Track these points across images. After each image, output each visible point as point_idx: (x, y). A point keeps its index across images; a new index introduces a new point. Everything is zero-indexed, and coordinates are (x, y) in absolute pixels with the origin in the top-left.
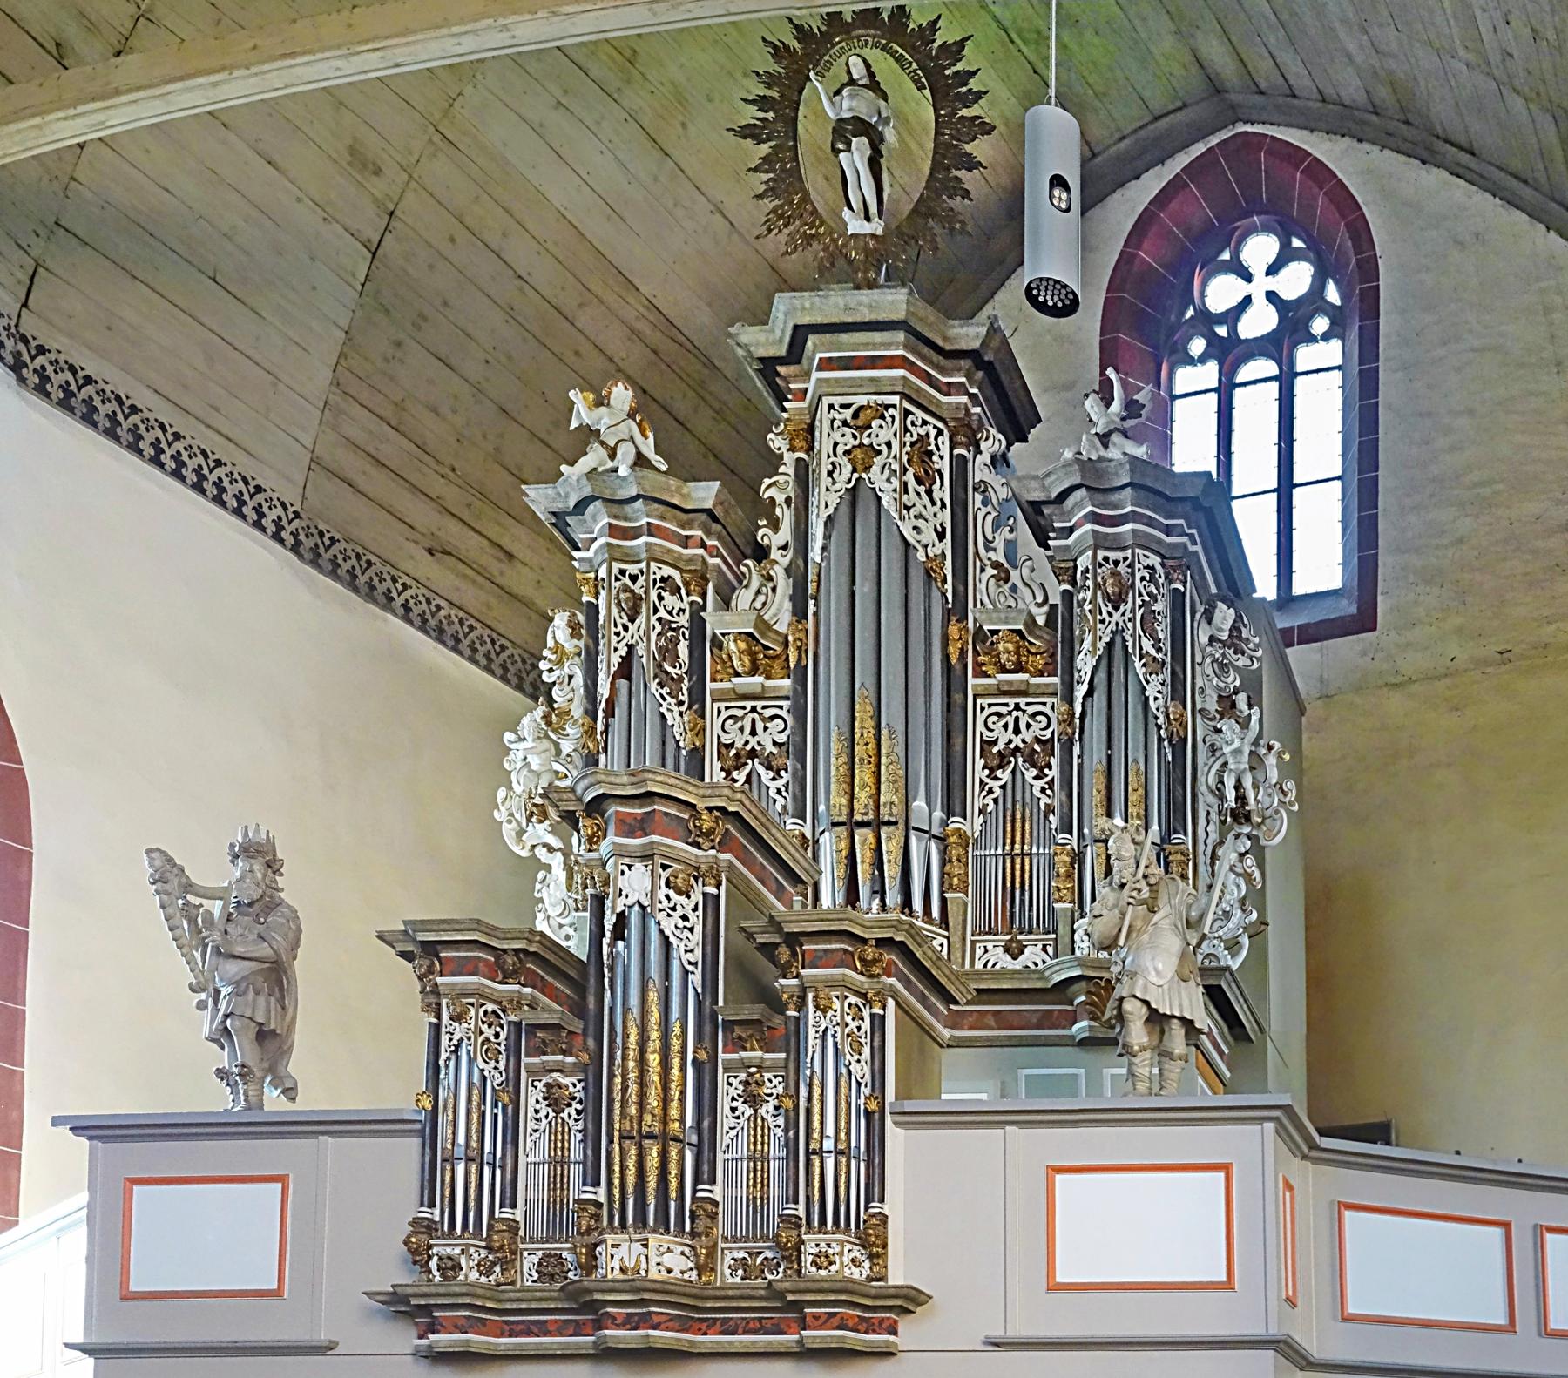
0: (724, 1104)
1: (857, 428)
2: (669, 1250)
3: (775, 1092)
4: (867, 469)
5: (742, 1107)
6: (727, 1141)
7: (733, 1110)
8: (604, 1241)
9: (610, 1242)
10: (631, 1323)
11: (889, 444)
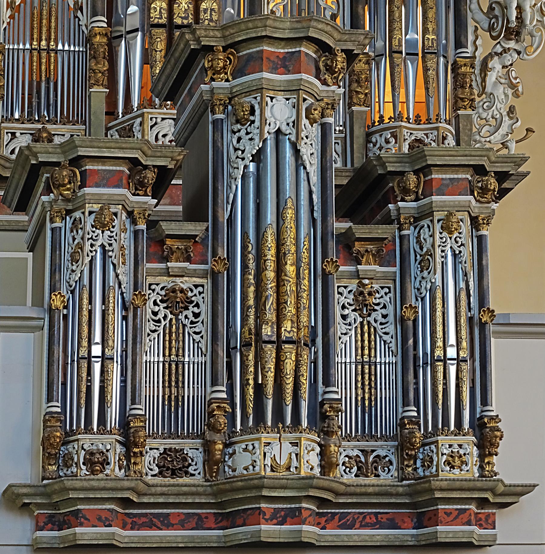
0: (338, 311)
5: (353, 315)
7: (344, 317)
10: (281, 518)
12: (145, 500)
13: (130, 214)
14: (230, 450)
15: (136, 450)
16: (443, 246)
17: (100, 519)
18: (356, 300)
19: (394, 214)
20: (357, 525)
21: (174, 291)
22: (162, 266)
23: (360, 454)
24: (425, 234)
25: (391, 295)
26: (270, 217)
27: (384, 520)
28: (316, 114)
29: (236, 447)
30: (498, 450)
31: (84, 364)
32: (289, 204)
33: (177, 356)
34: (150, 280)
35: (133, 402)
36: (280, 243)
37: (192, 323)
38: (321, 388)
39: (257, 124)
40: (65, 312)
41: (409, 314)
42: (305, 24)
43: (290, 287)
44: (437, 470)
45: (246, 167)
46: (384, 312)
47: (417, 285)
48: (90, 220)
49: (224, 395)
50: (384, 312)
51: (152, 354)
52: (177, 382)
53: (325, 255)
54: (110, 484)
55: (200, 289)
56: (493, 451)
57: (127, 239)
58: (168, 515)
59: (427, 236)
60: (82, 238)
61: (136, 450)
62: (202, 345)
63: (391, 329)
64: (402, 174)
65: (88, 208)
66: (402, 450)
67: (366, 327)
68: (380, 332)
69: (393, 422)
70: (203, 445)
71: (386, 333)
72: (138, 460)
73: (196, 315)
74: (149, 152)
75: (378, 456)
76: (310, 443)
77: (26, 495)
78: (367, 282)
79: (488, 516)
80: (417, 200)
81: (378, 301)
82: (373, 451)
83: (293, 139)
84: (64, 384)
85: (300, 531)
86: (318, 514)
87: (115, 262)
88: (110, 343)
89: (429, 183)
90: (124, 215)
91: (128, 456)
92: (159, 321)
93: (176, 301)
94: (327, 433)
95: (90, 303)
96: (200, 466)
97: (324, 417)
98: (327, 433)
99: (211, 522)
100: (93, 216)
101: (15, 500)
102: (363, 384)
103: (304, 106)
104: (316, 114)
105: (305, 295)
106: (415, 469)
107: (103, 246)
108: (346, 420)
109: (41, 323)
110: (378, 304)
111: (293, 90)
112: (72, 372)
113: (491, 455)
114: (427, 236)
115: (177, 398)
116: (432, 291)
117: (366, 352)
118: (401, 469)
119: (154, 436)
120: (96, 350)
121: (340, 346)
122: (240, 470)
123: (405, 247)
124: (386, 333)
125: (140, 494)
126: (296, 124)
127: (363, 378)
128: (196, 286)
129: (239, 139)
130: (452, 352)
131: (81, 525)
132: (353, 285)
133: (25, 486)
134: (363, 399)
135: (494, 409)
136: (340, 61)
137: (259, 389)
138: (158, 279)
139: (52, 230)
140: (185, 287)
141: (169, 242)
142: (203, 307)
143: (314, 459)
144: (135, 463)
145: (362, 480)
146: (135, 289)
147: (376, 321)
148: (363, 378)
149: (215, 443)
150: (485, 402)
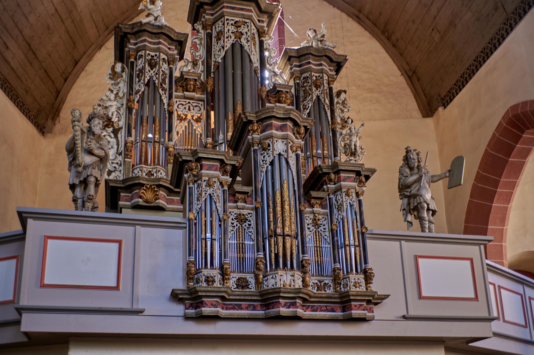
0: (306, 226)
5: (312, 228)
7: (309, 229)
8: (277, 273)
9: (280, 274)
12: (231, 297)
13: (221, 183)
14: (266, 279)
15: (227, 277)
16: (346, 201)
17: (212, 305)
18: (313, 222)
19: (326, 189)
20: (319, 310)
21: (240, 215)
22: (235, 205)
24: (339, 197)
25: (327, 221)
28: (294, 149)
29: (269, 277)
30: (373, 281)
31: (204, 241)
32: (285, 182)
33: (242, 241)
34: (230, 210)
35: (225, 258)
38: (301, 256)
39: (271, 150)
40: (195, 221)
41: (334, 227)
42: (289, 112)
43: (287, 214)
44: (350, 288)
45: (267, 167)
46: (324, 227)
47: (337, 217)
48: (204, 184)
49: (262, 256)
50: (324, 227)
51: (232, 241)
52: (243, 252)
53: (300, 203)
54: (216, 289)
55: (251, 215)
56: (371, 281)
57: (220, 193)
58: (241, 305)
59: (340, 198)
60: (201, 191)
61: (227, 277)
62: (252, 237)
63: (327, 234)
64: (328, 174)
65: (203, 178)
66: (335, 281)
67: (317, 233)
68: (323, 235)
69: (330, 270)
70: (255, 277)
72: (228, 281)
74: (228, 158)
75: (325, 283)
76: (298, 275)
77: (181, 294)
79: (370, 308)
80: (335, 184)
83: (286, 156)
84: (196, 251)
85: (296, 311)
86: (302, 306)
87: (215, 200)
88: (214, 233)
89: (339, 178)
90: (219, 184)
91: (223, 279)
92: (234, 227)
93: (241, 219)
94: (305, 273)
95: (205, 217)
96: (254, 285)
97: (303, 266)
98: (305, 273)
99: (259, 307)
100: (206, 182)
101: (175, 297)
102: (317, 255)
103: (290, 145)
104: (294, 149)
105: (293, 218)
106: (340, 288)
107: (210, 194)
108: (311, 268)
109: (185, 225)
112: (199, 244)
113: (370, 283)
114: (340, 198)
115: (243, 258)
116: (343, 219)
117: (318, 242)
118: (335, 288)
119: (234, 272)
120: (209, 235)
121: (307, 240)
122: (270, 286)
123: (331, 202)
125: (229, 295)
126: (287, 151)
127: (317, 253)
128: (249, 214)
129: (264, 157)
130: (352, 242)
131: (204, 307)
132: (312, 216)
133: (179, 290)
134: (318, 261)
135: (370, 266)
136: (302, 130)
137: (277, 255)
138: (233, 210)
139: (189, 188)
140: (244, 213)
141: (237, 195)
142: (252, 222)
143: (301, 283)
144: (226, 283)
145: (319, 292)
146: (224, 212)
148: (317, 253)
149: (259, 275)
150: (366, 263)
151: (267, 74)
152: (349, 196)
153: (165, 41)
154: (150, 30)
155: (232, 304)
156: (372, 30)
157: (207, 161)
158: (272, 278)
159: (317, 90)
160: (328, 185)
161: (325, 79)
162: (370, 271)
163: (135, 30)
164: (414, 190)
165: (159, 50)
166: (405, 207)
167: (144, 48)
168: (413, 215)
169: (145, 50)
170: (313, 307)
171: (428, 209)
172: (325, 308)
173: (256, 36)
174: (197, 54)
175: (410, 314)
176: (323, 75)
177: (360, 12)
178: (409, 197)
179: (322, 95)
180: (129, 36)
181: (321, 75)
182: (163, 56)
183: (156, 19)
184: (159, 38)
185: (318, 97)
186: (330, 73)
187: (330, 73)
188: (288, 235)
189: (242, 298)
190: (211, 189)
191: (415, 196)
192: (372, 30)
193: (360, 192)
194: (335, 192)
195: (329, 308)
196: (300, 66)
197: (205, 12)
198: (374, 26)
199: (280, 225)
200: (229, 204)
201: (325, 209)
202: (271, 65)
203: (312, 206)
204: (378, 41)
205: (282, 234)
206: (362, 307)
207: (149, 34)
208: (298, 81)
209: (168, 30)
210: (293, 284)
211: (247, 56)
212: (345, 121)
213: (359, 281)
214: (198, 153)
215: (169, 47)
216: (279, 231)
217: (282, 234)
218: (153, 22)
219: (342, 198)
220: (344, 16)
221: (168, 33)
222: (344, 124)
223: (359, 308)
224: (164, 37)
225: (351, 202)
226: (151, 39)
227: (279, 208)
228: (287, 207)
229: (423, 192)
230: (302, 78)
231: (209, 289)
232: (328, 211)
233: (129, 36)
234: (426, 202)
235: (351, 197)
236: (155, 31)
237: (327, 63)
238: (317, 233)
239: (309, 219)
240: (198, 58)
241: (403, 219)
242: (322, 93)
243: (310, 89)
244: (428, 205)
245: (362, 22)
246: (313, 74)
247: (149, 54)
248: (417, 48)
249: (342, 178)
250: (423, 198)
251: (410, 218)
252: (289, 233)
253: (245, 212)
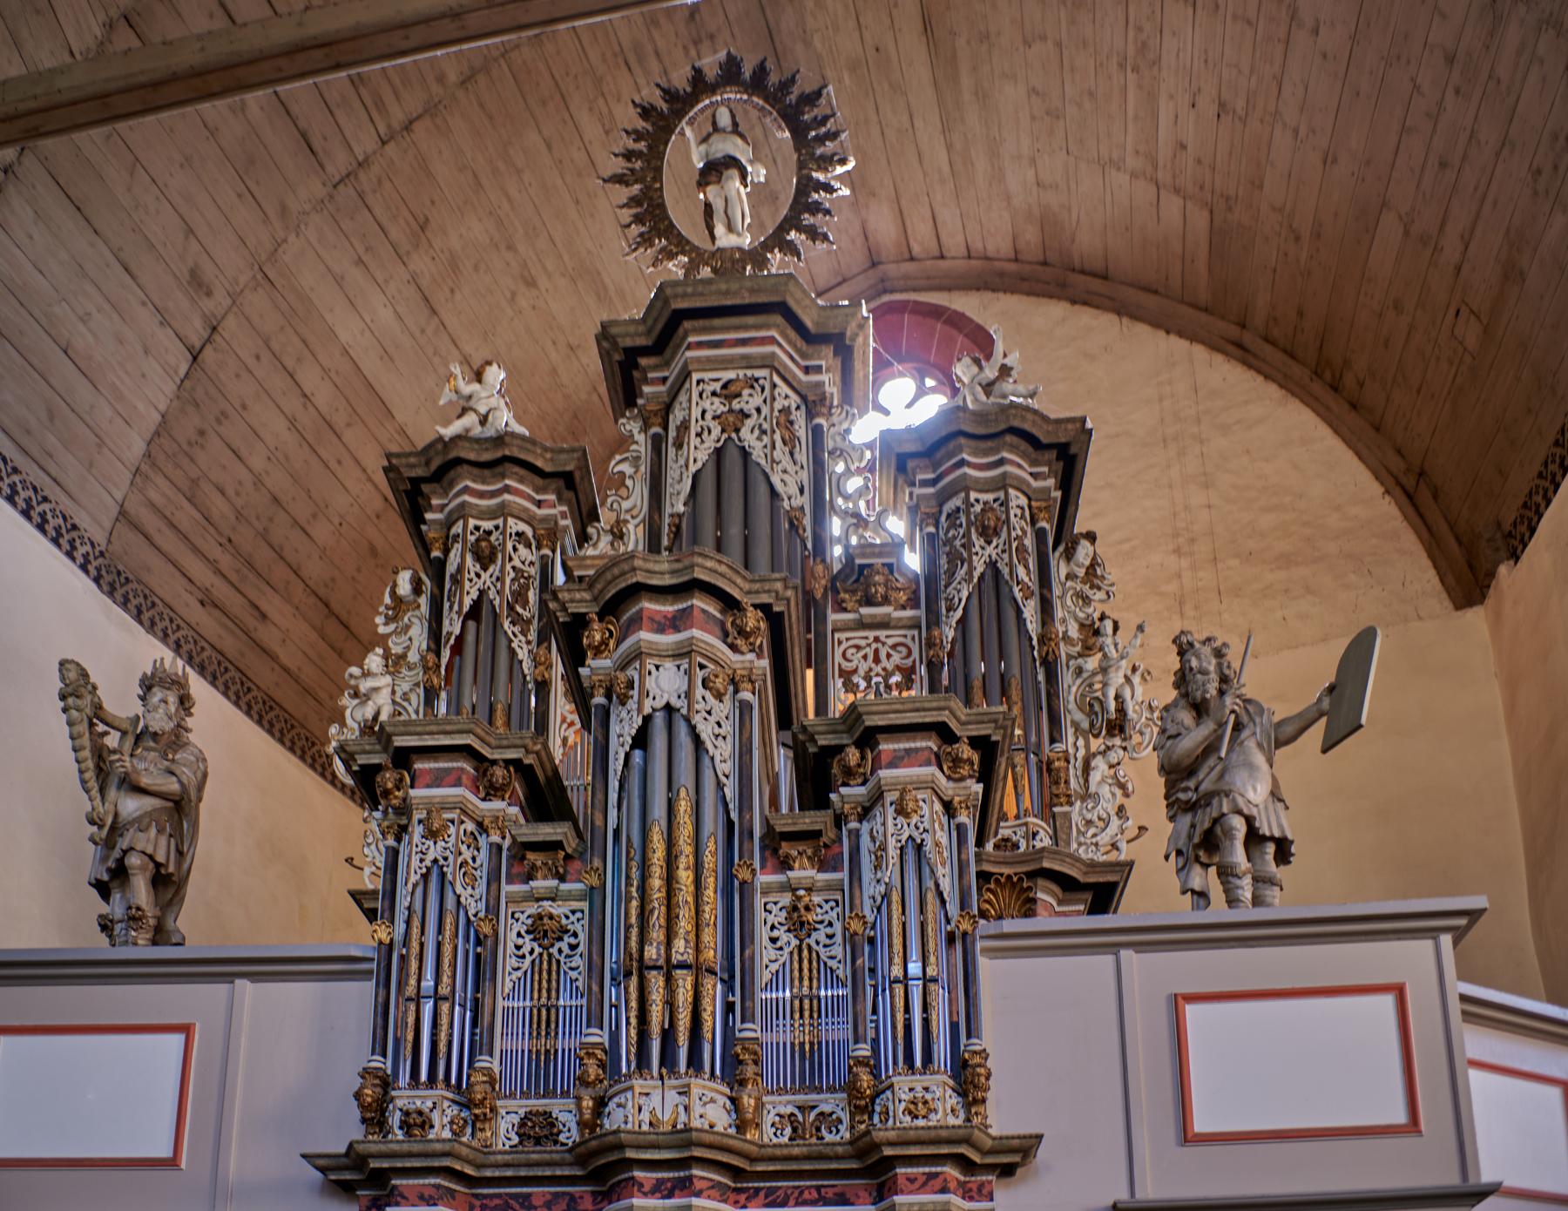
0: (762, 934)
1: (726, 397)
2: (712, 1101)
3: (827, 918)
4: (737, 430)
5: (784, 937)
6: (767, 976)
7: (774, 940)
8: (631, 1088)
9: (637, 1090)
11: (758, 410)
20: (792, 1202)
21: (540, 917)
22: (524, 888)
23: (796, 1111)
25: (839, 909)
26: (658, 811)
27: (830, 1195)
36: (670, 843)
37: (568, 956)
43: (685, 893)
50: (829, 931)
55: (579, 915)
62: (580, 984)
63: (838, 950)
67: (805, 953)
68: (823, 957)
71: (832, 958)
73: (573, 947)
75: (822, 1114)
78: (802, 892)
80: (863, 784)
81: (820, 918)
82: (813, 1107)
92: (523, 957)
110: (821, 922)
111: (683, 653)
117: (806, 983)
124: (832, 958)
125: (479, 1167)
128: (573, 912)
132: (786, 899)
140: (554, 912)
141: (531, 856)
147: (818, 943)
151: (836, 526)
152: (907, 816)
153: (521, 481)
154: (472, 456)
155: (499, 1196)
156: (1285, 375)
157: (429, 759)
158: (619, 1105)
159: (989, 543)
160: (843, 790)
161: (1013, 504)
162: (977, 1060)
163: (436, 463)
164: (1206, 779)
165: (502, 511)
166: (1181, 844)
167: (462, 512)
168: (1213, 870)
169: (465, 518)
170: (771, 1191)
171: (1254, 838)
172: (815, 1195)
173: (799, 418)
174: (626, 505)
175: (1139, 1195)
176: (1007, 494)
177: (1243, 326)
178: (1191, 807)
179: (1005, 556)
180: (425, 488)
181: (1001, 494)
182: (515, 526)
183: (484, 420)
184: (503, 476)
185: (992, 565)
186: (1035, 484)
187: (1035, 484)
188: (683, 966)
189: (523, 1173)
190: (441, 844)
191: (1206, 800)
192: (1285, 375)
193: (957, 799)
194: (865, 813)
195: (830, 1193)
196: (934, 482)
197: (646, 381)
198: (1290, 362)
199: (657, 934)
200: (506, 888)
201: (835, 870)
202: (847, 498)
203: (785, 865)
204: (1307, 405)
205: (661, 962)
206: (938, 1183)
207: (476, 471)
208: (932, 529)
209: (520, 447)
210: (683, 1118)
211: (761, 478)
212: (1091, 631)
213: (928, 1097)
214: (389, 736)
215: (538, 497)
216: (651, 952)
217: (661, 962)
218: (477, 431)
219: (884, 824)
220: (1199, 351)
221: (522, 456)
222: (1091, 641)
223: (925, 1184)
224: (516, 469)
225: (916, 834)
226: (484, 482)
227: (656, 882)
228: (685, 876)
229: (1239, 779)
230: (943, 518)
231: (416, 1147)
232: (844, 875)
233: (425, 488)
234: (1239, 812)
235: (915, 819)
236: (486, 457)
237: (1024, 456)
238: (805, 953)
239: (775, 909)
240: (628, 517)
241: (1176, 884)
242: (1004, 551)
243: (963, 546)
244: (1249, 820)
245: (1255, 356)
246: (973, 495)
247: (477, 528)
248: (1419, 391)
249: (884, 759)
250: (1234, 800)
251: (1197, 879)
252: (690, 958)
253: (558, 909)
